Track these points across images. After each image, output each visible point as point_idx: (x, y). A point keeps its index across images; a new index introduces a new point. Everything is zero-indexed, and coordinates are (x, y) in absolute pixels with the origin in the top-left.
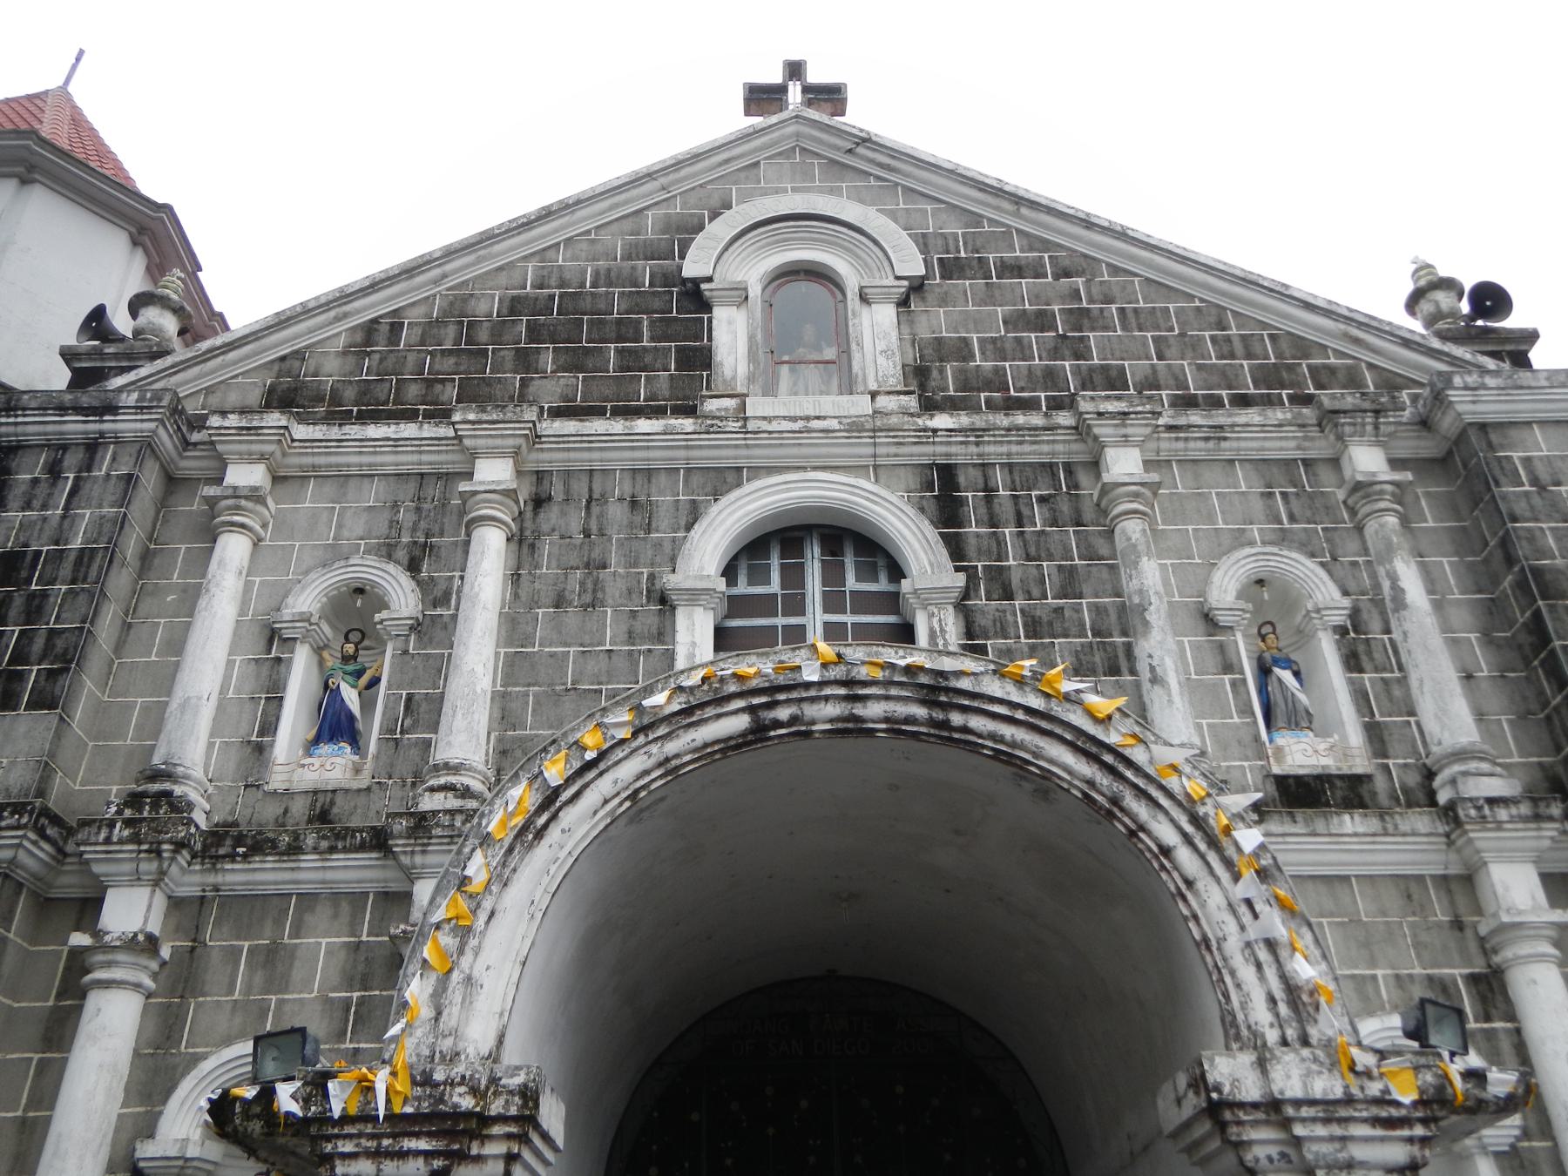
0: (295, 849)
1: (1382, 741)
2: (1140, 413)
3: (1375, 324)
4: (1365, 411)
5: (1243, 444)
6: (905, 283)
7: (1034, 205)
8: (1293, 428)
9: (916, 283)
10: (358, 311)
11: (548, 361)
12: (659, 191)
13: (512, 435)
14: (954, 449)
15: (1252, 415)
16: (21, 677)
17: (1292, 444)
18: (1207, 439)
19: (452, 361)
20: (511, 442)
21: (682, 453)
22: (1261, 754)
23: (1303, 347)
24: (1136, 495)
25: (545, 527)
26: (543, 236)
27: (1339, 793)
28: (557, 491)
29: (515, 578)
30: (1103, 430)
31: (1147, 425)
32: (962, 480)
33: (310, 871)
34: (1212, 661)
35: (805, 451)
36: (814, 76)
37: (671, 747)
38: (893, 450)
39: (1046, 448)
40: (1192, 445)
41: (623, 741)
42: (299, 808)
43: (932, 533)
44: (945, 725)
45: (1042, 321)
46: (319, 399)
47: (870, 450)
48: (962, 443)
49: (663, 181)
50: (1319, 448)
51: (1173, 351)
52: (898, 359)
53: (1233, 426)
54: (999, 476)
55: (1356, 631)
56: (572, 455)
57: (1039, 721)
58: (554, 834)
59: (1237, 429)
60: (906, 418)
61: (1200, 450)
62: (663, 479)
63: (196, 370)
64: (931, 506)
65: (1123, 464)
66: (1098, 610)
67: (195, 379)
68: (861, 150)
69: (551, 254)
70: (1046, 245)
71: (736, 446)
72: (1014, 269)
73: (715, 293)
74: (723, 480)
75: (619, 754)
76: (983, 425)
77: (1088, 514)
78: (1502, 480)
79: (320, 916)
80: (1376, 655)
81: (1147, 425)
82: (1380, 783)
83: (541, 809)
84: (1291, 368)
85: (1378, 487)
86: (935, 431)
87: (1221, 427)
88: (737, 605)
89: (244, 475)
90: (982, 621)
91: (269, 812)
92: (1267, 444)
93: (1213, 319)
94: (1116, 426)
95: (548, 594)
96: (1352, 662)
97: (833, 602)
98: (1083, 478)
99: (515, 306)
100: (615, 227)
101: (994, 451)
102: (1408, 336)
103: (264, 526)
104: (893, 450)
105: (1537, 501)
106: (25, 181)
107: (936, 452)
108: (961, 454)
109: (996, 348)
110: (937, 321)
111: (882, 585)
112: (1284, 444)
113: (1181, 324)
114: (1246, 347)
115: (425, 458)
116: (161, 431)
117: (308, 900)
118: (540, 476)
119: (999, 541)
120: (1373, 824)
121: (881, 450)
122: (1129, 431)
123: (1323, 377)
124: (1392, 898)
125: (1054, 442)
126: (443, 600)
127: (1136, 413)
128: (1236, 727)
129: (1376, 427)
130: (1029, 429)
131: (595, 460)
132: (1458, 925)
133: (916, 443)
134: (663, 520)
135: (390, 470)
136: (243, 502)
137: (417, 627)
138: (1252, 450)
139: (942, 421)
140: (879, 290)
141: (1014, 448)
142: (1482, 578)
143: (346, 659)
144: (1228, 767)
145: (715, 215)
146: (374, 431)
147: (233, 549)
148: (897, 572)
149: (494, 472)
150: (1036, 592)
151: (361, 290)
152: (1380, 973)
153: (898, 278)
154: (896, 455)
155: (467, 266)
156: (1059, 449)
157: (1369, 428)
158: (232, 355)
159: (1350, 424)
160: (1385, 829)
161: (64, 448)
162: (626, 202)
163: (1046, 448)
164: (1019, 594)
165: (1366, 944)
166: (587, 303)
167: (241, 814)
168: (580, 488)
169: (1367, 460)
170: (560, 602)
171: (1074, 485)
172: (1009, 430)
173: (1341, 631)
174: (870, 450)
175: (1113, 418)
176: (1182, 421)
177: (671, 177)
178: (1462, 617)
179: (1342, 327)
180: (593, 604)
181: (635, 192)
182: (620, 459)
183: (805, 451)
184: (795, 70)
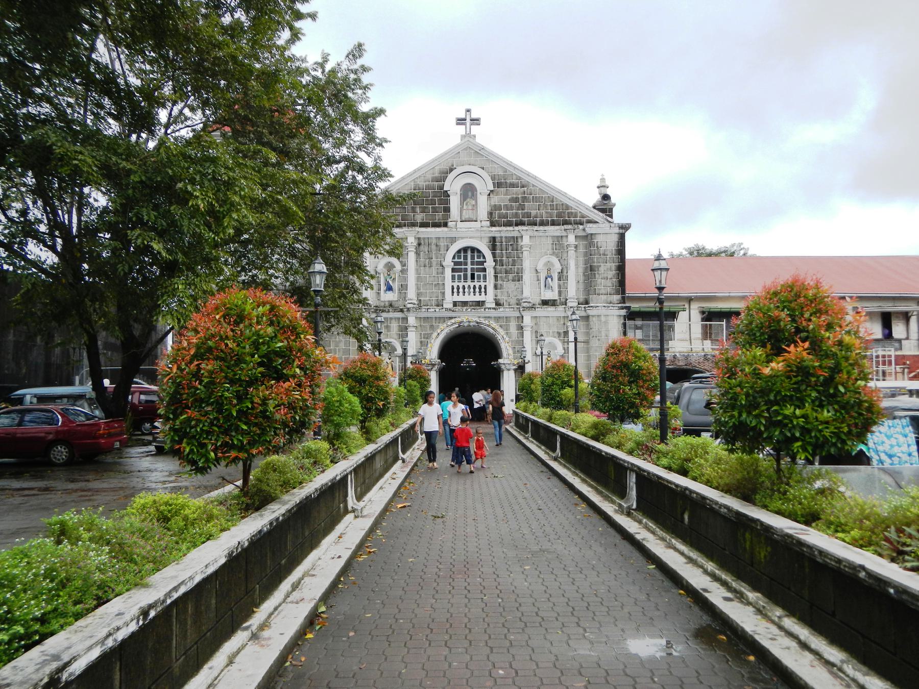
0: (389, 312)
11: (418, 210)
13: (414, 234)
15: (553, 228)
23: (568, 207)
28: (422, 242)
30: (523, 233)
33: (391, 315)
34: (536, 279)
36: (474, 116)
42: (387, 304)
43: (490, 252)
45: (516, 200)
50: (564, 234)
51: (542, 208)
54: (504, 240)
57: (489, 326)
62: (442, 240)
64: (491, 248)
65: (526, 240)
66: (518, 269)
70: (520, 178)
72: (513, 185)
74: (453, 240)
77: (519, 248)
79: (393, 321)
82: (558, 301)
84: (564, 213)
88: (456, 263)
90: (498, 271)
91: (382, 304)
95: (423, 265)
96: (559, 279)
97: (472, 263)
98: (519, 240)
101: (503, 235)
107: (492, 235)
108: (497, 235)
109: (507, 207)
110: (495, 200)
111: (482, 259)
113: (545, 201)
117: (391, 319)
118: (419, 239)
119: (502, 253)
123: (570, 214)
124: (555, 320)
126: (404, 265)
131: (429, 236)
132: (564, 324)
134: (442, 249)
137: (401, 271)
139: (494, 229)
142: (586, 262)
143: (389, 275)
145: (451, 170)
148: (484, 257)
149: (411, 241)
156: (515, 234)
167: (378, 305)
168: (426, 241)
169: (571, 239)
170: (425, 266)
171: (517, 242)
173: (559, 273)
178: (581, 270)
180: (431, 266)
182: (433, 236)
184: (468, 111)
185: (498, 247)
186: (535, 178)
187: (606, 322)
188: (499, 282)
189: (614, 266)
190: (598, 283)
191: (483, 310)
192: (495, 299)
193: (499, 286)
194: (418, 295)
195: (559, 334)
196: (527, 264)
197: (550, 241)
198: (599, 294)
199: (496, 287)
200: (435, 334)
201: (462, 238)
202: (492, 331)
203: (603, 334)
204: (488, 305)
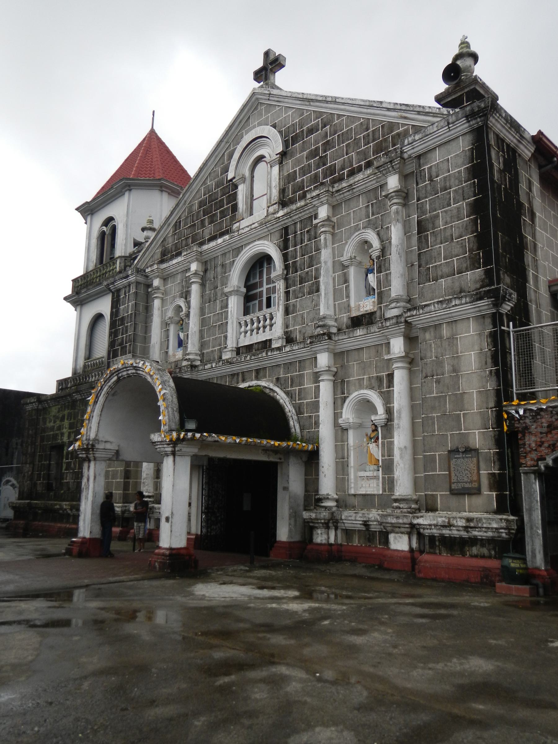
1: (382, 298)
2: (322, 193)
3: (408, 109)
4: (387, 163)
5: (360, 188)
6: (278, 156)
7: (312, 100)
8: (372, 176)
9: (283, 153)
10: (172, 221)
12: (226, 144)
14: (286, 221)
16: (126, 346)
17: (374, 182)
18: (349, 191)
19: (190, 230)
20: (194, 257)
21: (229, 246)
22: (349, 311)
23: (392, 126)
24: (323, 226)
25: (207, 279)
26: (203, 176)
27: (366, 320)
29: (202, 296)
31: (326, 196)
32: (289, 231)
34: (342, 279)
35: (253, 235)
37: (109, 384)
38: (272, 227)
39: (307, 212)
40: (345, 194)
41: (103, 384)
42: (173, 365)
44: (137, 373)
46: (169, 252)
47: (266, 230)
48: (287, 219)
49: (225, 140)
51: (351, 149)
52: (278, 188)
53: (354, 183)
55: (382, 257)
56: (210, 255)
58: (99, 402)
59: (356, 183)
60: (273, 216)
61: (349, 195)
63: (147, 253)
64: (282, 245)
65: (323, 212)
67: (149, 254)
68: (271, 98)
69: (206, 181)
71: (239, 240)
72: (311, 131)
73: (237, 182)
74: (238, 250)
75: (104, 386)
76: (289, 211)
78: (419, 181)
80: (386, 265)
81: (326, 196)
83: (96, 397)
85: (390, 195)
86: (279, 217)
87: (351, 185)
89: (156, 282)
92: (367, 185)
93: (365, 127)
94: (318, 200)
99: (201, 204)
100: (218, 164)
102: (418, 109)
103: (163, 295)
104: (272, 227)
105: (429, 188)
106: (130, 190)
108: (289, 222)
109: (304, 171)
112: (372, 183)
114: (373, 136)
115: (185, 265)
116: (138, 278)
119: (296, 250)
120: (365, 330)
121: (270, 229)
122: (322, 200)
125: (308, 209)
127: (321, 193)
128: (344, 302)
129: (393, 167)
130: (301, 207)
133: (276, 223)
135: (180, 271)
136: (155, 291)
138: (363, 189)
140: (272, 162)
141: (300, 215)
144: (341, 317)
146: (175, 261)
147: (157, 303)
150: (303, 268)
151: (170, 215)
152: (365, 377)
153: (277, 155)
154: (273, 229)
155: (189, 196)
157: (390, 169)
158: (153, 246)
159: (384, 170)
160: (367, 332)
161: (126, 287)
162: (219, 153)
163: (307, 212)
164: (299, 270)
165: (364, 369)
166: (213, 198)
172: (296, 210)
174: (266, 230)
175: (316, 198)
176: (340, 188)
177: (227, 138)
179: (400, 114)
181: (219, 149)
183: (253, 235)
185: (291, 243)
186: (334, 101)
187: (452, 339)
188: (292, 301)
189: (464, 205)
190: (435, 254)
191: (264, 354)
192: (286, 333)
193: (291, 308)
194: (203, 345)
195: (379, 379)
196: (325, 255)
197: (362, 203)
198: (436, 279)
199: (287, 312)
200: (91, 399)
201: (249, 244)
202: (149, 379)
203: (447, 368)
204: (275, 345)
